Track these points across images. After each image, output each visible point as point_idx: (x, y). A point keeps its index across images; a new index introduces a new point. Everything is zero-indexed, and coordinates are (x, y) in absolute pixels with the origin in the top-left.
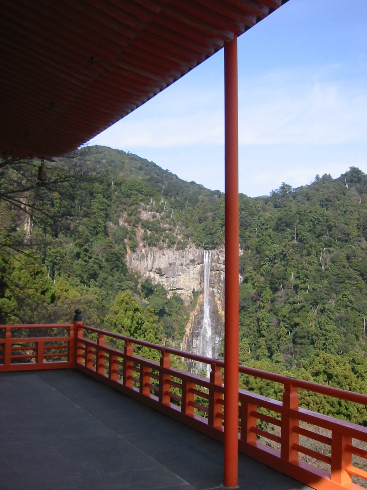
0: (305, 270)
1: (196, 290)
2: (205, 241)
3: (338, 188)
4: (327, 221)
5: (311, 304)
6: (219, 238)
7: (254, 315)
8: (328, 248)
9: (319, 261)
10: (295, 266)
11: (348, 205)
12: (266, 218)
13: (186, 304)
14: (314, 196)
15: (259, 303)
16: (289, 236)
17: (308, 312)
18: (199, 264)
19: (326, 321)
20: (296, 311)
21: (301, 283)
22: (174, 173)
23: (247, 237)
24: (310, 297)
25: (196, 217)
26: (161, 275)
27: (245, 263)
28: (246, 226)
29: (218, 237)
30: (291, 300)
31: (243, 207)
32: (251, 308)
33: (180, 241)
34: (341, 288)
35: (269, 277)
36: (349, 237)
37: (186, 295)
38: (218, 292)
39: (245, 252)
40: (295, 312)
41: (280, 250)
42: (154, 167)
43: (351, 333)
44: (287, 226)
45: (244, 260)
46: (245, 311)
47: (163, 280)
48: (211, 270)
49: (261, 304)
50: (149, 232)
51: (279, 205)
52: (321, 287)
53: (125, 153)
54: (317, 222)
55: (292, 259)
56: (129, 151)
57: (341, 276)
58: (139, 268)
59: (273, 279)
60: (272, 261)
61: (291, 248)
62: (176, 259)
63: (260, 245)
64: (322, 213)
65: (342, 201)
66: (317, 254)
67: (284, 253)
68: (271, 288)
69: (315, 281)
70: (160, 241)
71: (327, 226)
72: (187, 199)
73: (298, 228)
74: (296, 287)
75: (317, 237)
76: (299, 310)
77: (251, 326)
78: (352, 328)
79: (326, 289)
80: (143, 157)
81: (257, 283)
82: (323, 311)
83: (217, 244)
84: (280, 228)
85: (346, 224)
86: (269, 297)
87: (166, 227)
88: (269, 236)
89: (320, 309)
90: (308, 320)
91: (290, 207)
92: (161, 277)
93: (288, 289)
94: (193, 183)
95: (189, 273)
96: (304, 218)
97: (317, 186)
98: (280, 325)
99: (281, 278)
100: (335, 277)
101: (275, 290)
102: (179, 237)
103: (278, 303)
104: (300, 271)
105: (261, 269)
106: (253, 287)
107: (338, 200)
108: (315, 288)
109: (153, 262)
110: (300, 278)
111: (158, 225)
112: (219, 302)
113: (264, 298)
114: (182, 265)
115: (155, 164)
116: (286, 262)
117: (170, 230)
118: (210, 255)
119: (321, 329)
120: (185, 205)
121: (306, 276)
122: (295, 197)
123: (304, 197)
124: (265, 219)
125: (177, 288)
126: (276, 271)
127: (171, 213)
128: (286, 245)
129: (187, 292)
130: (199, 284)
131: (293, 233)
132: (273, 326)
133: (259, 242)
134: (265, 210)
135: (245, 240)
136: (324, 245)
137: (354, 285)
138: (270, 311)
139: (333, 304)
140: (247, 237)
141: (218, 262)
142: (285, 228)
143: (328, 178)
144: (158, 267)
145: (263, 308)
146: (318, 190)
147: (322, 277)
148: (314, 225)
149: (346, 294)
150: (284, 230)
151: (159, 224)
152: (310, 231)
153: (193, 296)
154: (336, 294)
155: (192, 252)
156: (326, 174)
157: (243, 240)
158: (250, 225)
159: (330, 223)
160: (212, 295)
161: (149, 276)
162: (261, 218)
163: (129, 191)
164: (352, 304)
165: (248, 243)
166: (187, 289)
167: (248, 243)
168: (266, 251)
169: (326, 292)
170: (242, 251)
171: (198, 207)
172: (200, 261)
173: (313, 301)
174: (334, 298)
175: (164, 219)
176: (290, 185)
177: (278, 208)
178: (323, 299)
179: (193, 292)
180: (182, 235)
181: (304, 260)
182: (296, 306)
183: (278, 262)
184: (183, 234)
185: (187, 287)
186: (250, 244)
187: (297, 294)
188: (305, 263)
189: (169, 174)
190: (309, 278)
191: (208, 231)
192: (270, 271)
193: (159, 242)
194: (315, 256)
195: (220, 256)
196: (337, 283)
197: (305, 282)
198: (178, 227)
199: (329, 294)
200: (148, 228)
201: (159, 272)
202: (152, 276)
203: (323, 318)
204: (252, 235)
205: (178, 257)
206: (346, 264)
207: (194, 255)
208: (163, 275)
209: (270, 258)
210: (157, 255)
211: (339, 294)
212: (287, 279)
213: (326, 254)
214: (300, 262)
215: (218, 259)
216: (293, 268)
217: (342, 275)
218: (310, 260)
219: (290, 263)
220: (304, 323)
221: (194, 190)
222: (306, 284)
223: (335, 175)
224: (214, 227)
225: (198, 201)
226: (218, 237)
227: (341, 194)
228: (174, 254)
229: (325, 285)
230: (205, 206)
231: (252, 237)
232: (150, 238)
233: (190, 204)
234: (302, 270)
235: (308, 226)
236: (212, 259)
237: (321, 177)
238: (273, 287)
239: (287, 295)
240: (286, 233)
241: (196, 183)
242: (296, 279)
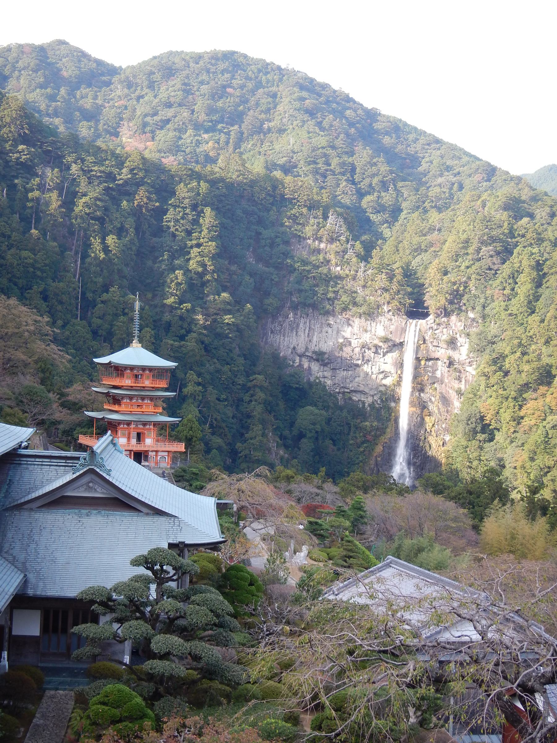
47: (325, 373)
92: (322, 367)
115: (347, 96)
125: (353, 389)
144: (317, 349)
161: (300, 365)
163: (268, 198)
166: (372, 393)
185: (371, 389)
202: (306, 365)
207: (385, 327)
208: (325, 365)
210: (316, 326)
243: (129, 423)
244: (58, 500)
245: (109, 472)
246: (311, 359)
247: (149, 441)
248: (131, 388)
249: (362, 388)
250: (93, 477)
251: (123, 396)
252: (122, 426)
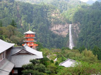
109: (55, 28)
114: (63, 28)
172: (68, 27)
208: (58, 32)
244: (19, 54)
245: (26, 49)
246: (56, 31)
247: (32, 45)
248: (29, 37)
250: (23, 50)
251: (28, 38)
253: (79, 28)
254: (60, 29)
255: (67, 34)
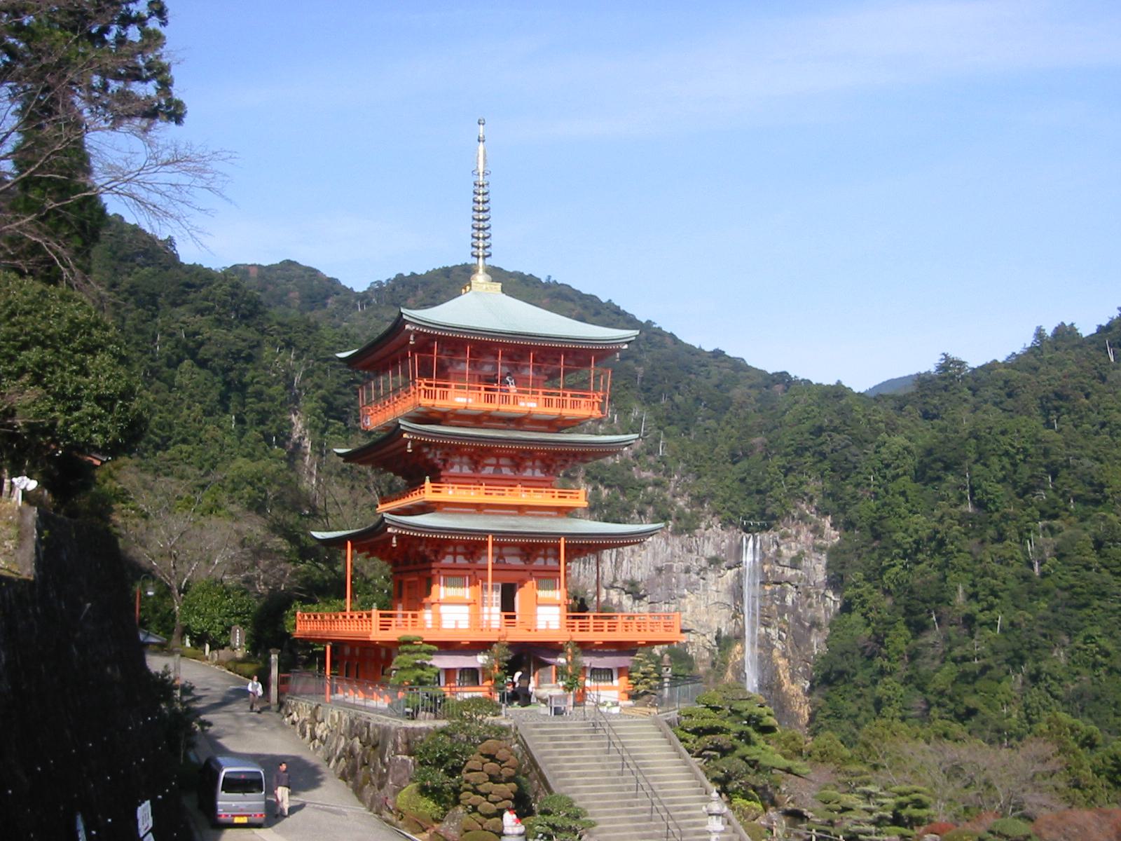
0: (989, 578)
1: (724, 632)
2: (746, 510)
3: (1086, 364)
4: (1046, 453)
5: (1007, 661)
6: (778, 503)
7: (865, 691)
8: (1049, 522)
9: (1026, 553)
10: (967, 567)
11: (1111, 409)
12: (895, 449)
13: (701, 669)
14: (1025, 387)
15: (878, 662)
16: (951, 495)
17: (999, 682)
18: (730, 568)
19: (1043, 701)
20: (970, 679)
21: (982, 611)
22: (667, 329)
23: (847, 497)
24: (1002, 645)
25: (723, 449)
26: (638, 597)
27: (844, 563)
28: (845, 470)
29: (777, 500)
30: (957, 652)
31: (837, 422)
32: (860, 674)
33: (681, 511)
34: (1082, 620)
35: (903, 597)
36: (1102, 492)
37: (700, 645)
38: (780, 638)
39: (845, 535)
40: (968, 683)
41: (929, 528)
42: (615, 317)
43: (1109, 732)
44: (947, 468)
45: (843, 556)
46: (845, 682)
47: (641, 609)
48: (761, 583)
49: (886, 663)
50: (605, 492)
51: (935, 412)
52: (1031, 617)
53: (539, 280)
54: (1022, 457)
55: (959, 551)
56: (549, 277)
57: (1079, 590)
58: (581, 581)
59: (914, 602)
60: (910, 556)
61: (957, 522)
62: (673, 555)
63: (881, 518)
64: (1035, 435)
65: (1095, 397)
66: (1022, 537)
67: (939, 536)
68: (908, 624)
69: (1017, 603)
70: (631, 513)
71: (1046, 467)
72: (702, 401)
73: (975, 472)
74: (969, 620)
75: (1020, 496)
76: (976, 678)
77: (860, 720)
78: (1111, 718)
79: (1043, 623)
80: (585, 291)
81: (874, 612)
82: (1035, 678)
83: (774, 517)
84: (930, 473)
85: (1097, 459)
86: (903, 647)
87: (647, 478)
88: (903, 494)
89: (1030, 673)
90: (1000, 700)
91: (954, 420)
93: (951, 625)
94: (718, 354)
95: (705, 590)
96: (988, 447)
97: (1032, 360)
98: (932, 713)
99: (933, 598)
100: (1066, 595)
101: (919, 628)
102: (681, 502)
103: (926, 660)
104: (978, 579)
105: (884, 578)
106: (866, 621)
107: (1087, 396)
108: (1016, 621)
110: (981, 597)
111: (627, 473)
112: (782, 662)
113: (891, 648)
114: (687, 571)
116: (944, 559)
117: (657, 484)
118: (758, 546)
119: (1031, 722)
120: (696, 417)
121: (994, 593)
122: (978, 390)
123: (1000, 388)
124: (891, 452)
126: (918, 581)
127: (657, 441)
128: (942, 517)
129: (702, 638)
130: (733, 618)
131: (961, 486)
132: (916, 717)
133: (878, 509)
134: (892, 429)
135: (845, 504)
136: (1037, 514)
137: (1114, 611)
138: (909, 679)
139: (1063, 661)
140: (847, 497)
141: (777, 562)
142: (942, 473)
143: (1069, 333)
144: (628, 577)
145: (890, 674)
146: (1036, 369)
147: (1034, 594)
148: (1014, 465)
149: (1094, 634)
150: (939, 478)
151: (629, 469)
152: (1004, 479)
153: (717, 649)
154: (1069, 635)
155: (713, 538)
156: (1063, 323)
157: (839, 505)
158: (855, 468)
159: (1054, 457)
160: (765, 644)
162: (883, 450)
164: (1108, 659)
165: (852, 513)
166: (703, 631)
167: (852, 513)
168: (895, 532)
169: (1044, 631)
170: (837, 533)
171: (728, 423)
173: (1011, 654)
174: (1064, 646)
175: (641, 459)
176: (963, 360)
177: (932, 419)
178: (1037, 647)
179: (717, 638)
180: (686, 495)
181: (987, 553)
182: (967, 667)
183: (924, 560)
184: (690, 495)
185: (702, 627)
186: (855, 515)
187: (973, 638)
188: (989, 560)
189: (655, 333)
190: (999, 597)
191: (752, 484)
192: (907, 581)
193: (628, 516)
194: (1015, 541)
195: (782, 548)
196: (1070, 607)
197: (991, 607)
198: (676, 477)
199: (1051, 636)
200: (602, 481)
201: (630, 589)
202: (615, 601)
203: (1036, 696)
204: (860, 494)
205: (677, 551)
206: (1093, 559)
207: (717, 546)
208: (641, 598)
209: (905, 550)
211: (1076, 635)
212: (948, 602)
213: (1044, 536)
214: (979, 558)
215: (778, 553)
216: (961, 573)
217: (1081, 587)
218: (1002, 552)
219: (955, 561)
220: (989, 707)
221: (721, 373)
222: (994, 612)
223: (1086, 329)
224: (767, 475)
225: (731, 404)
226: (777, 500)
227: (1094, 378)
228: (667, 544)
229: (1041, 613)
230: (745, 419)
231: (861, 499)
232: (608, 506)
233: (711, 412)
234: (982, 577)
235: (998, 467)
236: (763, 555)
237: (1049, 332)
238: (912, 621)
239: (947, 639)
240: (944, 485)
241: (727, 353)
242: (968, 600)
243: (472, 546)
248: (478, 419)
249: (689, 626)
251: (452, 449)
252: (448, 560)
253: (828, 567)
254: (659, 570)
255: (722, 622)
